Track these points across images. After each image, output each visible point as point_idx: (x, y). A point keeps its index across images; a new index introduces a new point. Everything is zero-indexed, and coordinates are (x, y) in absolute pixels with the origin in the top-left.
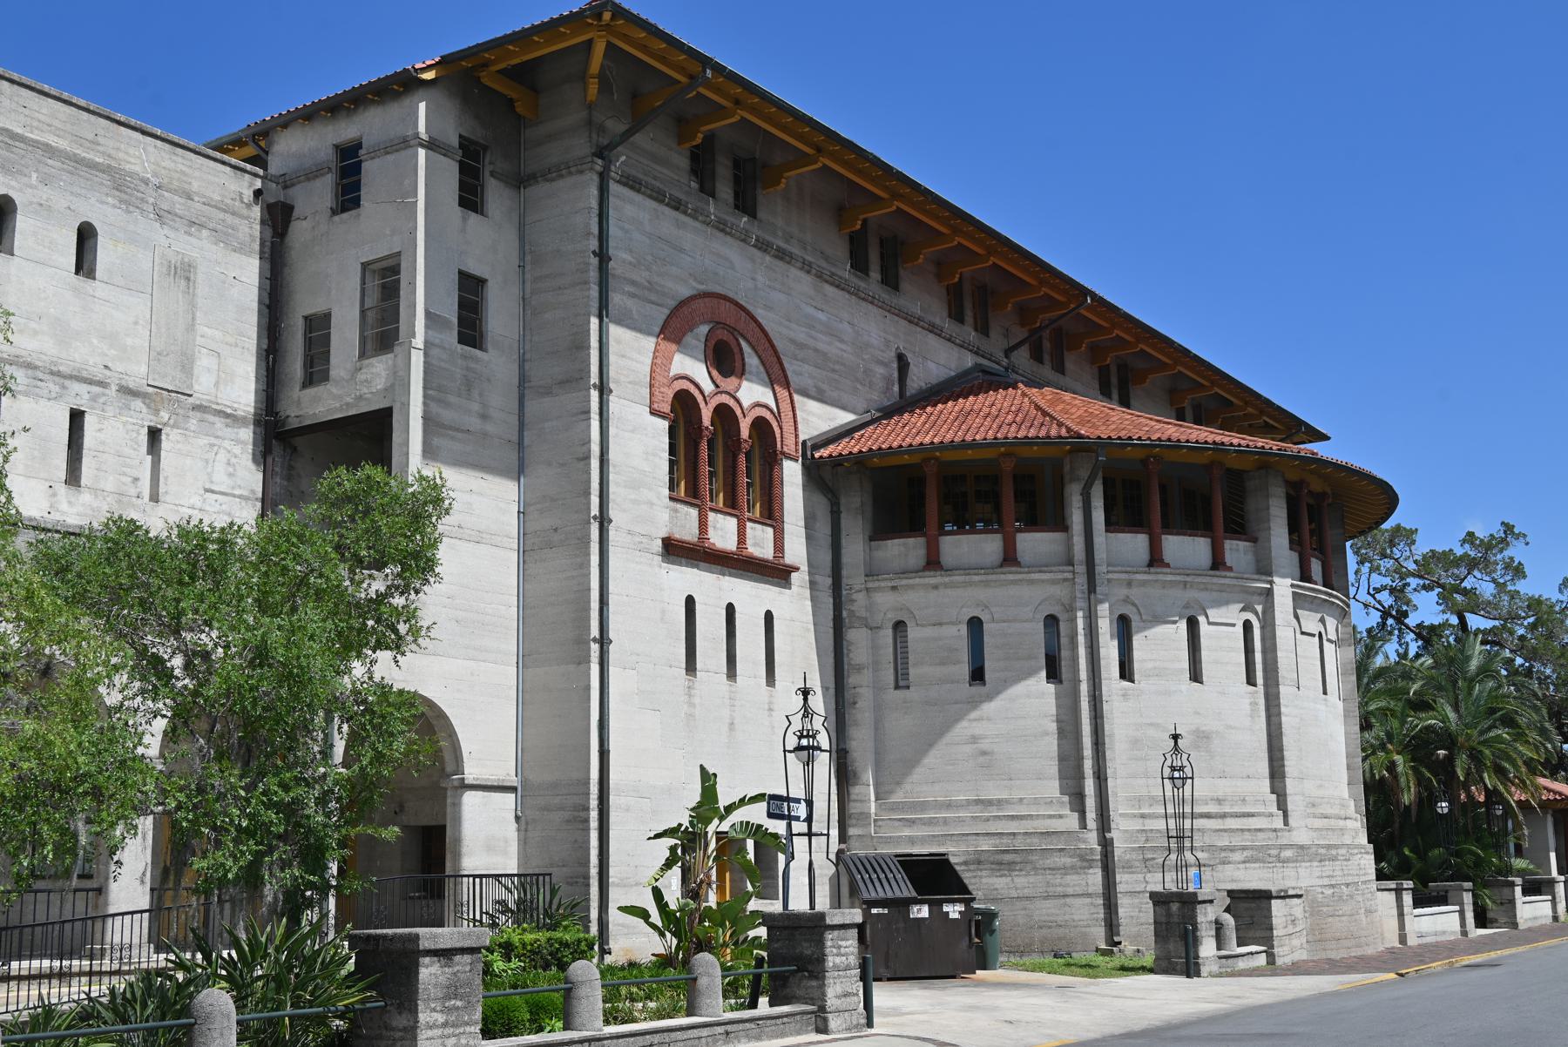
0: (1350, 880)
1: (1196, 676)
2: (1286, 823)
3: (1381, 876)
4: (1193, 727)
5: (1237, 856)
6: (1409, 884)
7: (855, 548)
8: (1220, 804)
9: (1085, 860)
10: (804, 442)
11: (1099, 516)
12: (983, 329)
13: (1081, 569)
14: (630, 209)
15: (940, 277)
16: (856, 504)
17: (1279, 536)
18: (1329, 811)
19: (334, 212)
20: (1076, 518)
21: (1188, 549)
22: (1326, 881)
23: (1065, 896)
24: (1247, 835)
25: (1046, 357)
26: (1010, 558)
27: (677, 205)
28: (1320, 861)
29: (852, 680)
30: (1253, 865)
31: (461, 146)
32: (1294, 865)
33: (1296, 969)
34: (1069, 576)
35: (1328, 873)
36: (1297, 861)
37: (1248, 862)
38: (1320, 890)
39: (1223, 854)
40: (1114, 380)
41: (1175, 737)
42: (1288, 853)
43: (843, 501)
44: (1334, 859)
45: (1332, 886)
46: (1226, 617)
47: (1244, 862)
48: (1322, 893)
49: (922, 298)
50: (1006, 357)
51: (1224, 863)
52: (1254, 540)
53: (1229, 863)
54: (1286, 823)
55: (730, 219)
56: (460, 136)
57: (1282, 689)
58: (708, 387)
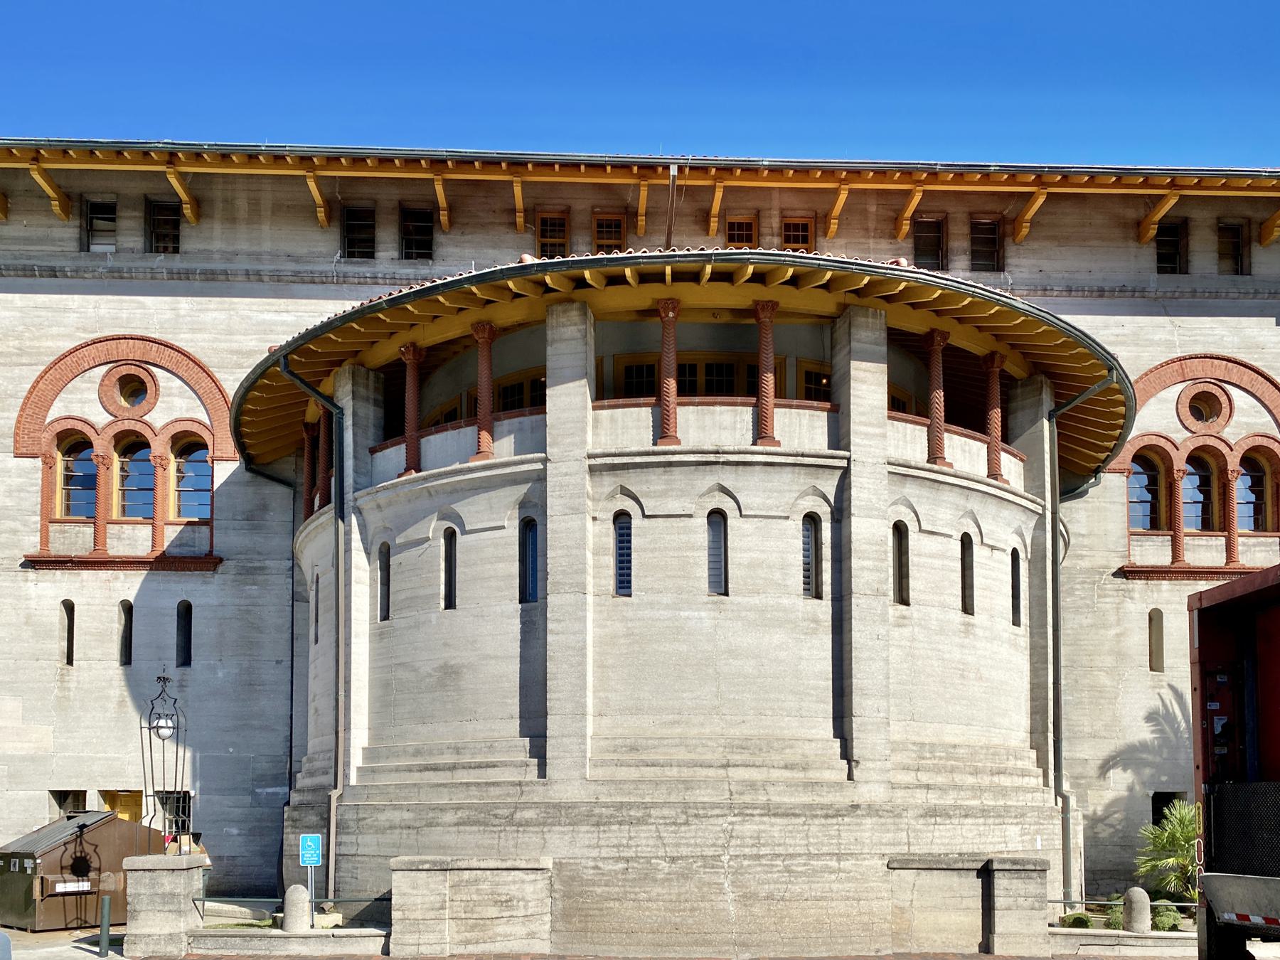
0: (684, 851)
2: (542, 773)
4: (441, 662)
5: (449, 817)
8: (458, 753)
22: (604, 852)
24: (474, 791)
28: (598, 824)
30: (468, 828)
32: (536, 829)
35: (616, 842)
36: (544, 824)
37: (464, 824)
38: (591, 864)
39: (431, 815)
42: (529, 814)
44: (641, 821)
45: (627, 860)
46: (488, 520)
47: (457, 824)
48: (596, 867)
51: (430, 825)
53: (438, 825)
54: (542, 773)
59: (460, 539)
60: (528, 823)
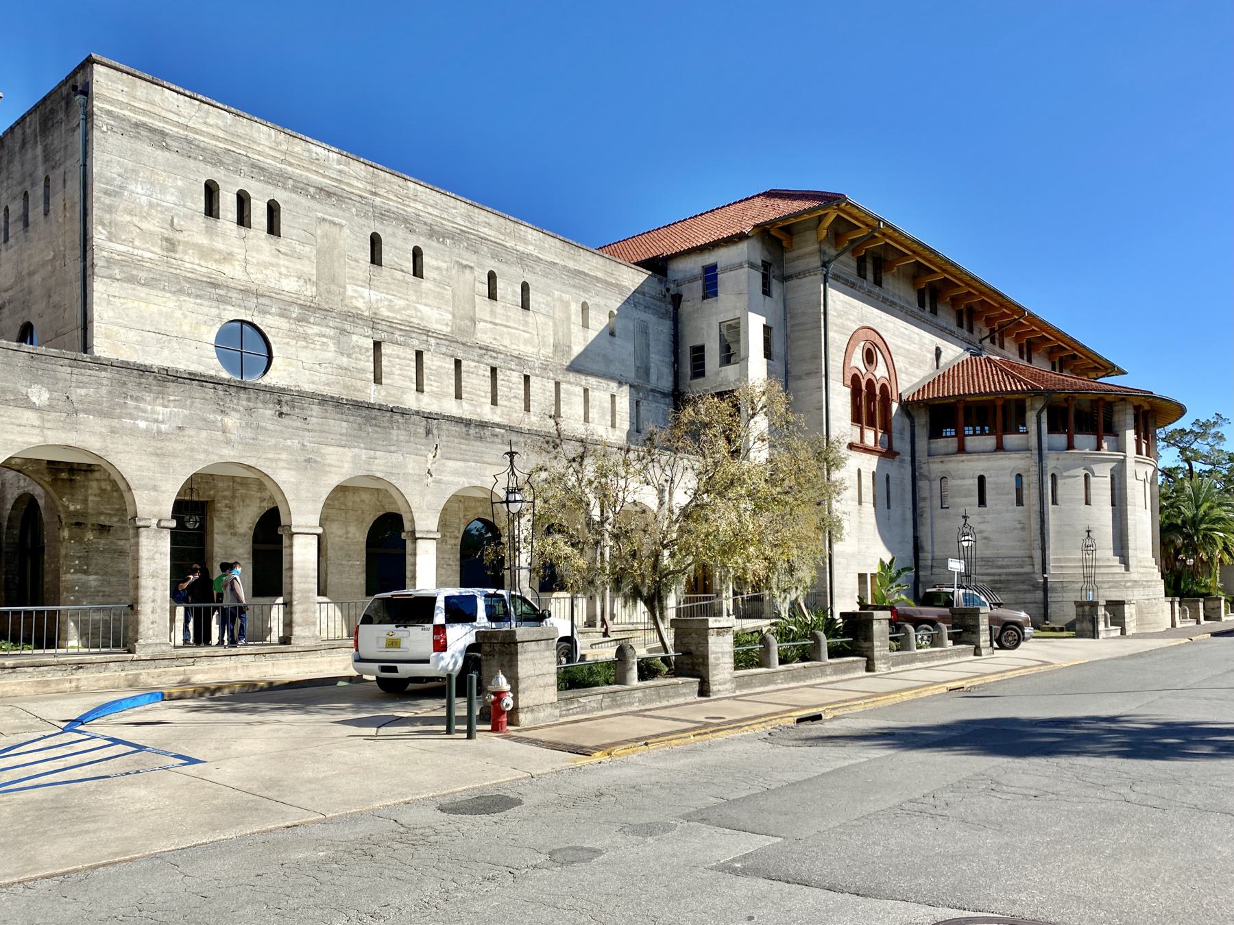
1: (1087, 502)
2: (1127, 569)
3: (1166, 595)
5: (1106, 585)
6: (1177, 599)
7: (922, 443)
9: (1035, 587)
10: (900, 394)
11: (1045, 427)
12: (971, 330)
13: (1036, 452)
14: (832, 292)
15: (953, 306)
16: (922, 420)
17: (1130, 436)
18: (1146, 564)
19: (704, 298)
20: (1033, 427)
21: (1085, 442)
22: (1146, 597)
23: (1025, 603)
25: (997, 341)
26: (1000, 447)
27: (853, 286)
29: (921, 504)
31: (763, 265)
33: (1135, 636)
34: (1029, 455)
40: (1025, 350)
41: (1089, 532)
42: (1129, 584)
43: (916, 421)
44: (1150, 587)
49: (947, 317)
50: (980, 343)
52: (1117, 435)
55: (872, 289)
56: (762, 261)
57: (1128, 507)
58: (864, 371)
59: (1092, 479)
60: (1129, 587)
